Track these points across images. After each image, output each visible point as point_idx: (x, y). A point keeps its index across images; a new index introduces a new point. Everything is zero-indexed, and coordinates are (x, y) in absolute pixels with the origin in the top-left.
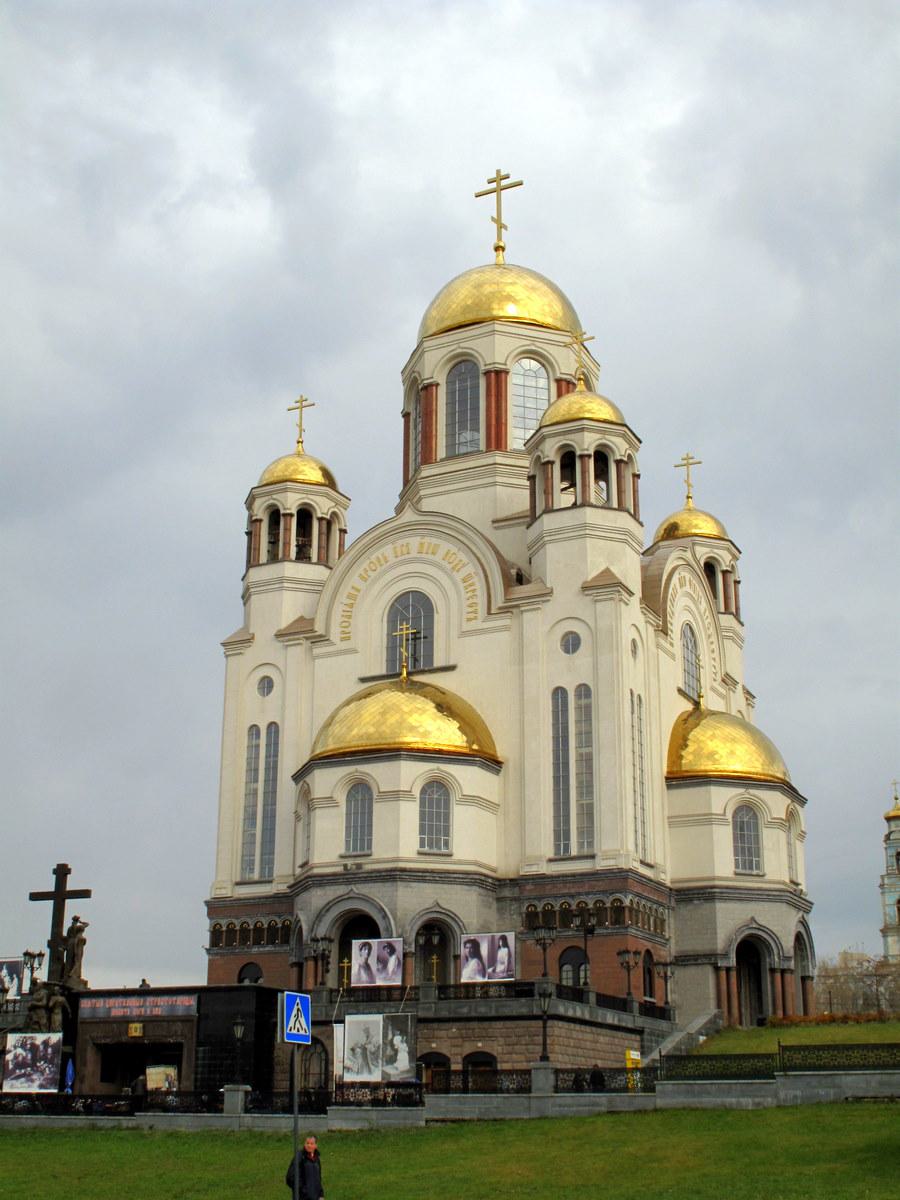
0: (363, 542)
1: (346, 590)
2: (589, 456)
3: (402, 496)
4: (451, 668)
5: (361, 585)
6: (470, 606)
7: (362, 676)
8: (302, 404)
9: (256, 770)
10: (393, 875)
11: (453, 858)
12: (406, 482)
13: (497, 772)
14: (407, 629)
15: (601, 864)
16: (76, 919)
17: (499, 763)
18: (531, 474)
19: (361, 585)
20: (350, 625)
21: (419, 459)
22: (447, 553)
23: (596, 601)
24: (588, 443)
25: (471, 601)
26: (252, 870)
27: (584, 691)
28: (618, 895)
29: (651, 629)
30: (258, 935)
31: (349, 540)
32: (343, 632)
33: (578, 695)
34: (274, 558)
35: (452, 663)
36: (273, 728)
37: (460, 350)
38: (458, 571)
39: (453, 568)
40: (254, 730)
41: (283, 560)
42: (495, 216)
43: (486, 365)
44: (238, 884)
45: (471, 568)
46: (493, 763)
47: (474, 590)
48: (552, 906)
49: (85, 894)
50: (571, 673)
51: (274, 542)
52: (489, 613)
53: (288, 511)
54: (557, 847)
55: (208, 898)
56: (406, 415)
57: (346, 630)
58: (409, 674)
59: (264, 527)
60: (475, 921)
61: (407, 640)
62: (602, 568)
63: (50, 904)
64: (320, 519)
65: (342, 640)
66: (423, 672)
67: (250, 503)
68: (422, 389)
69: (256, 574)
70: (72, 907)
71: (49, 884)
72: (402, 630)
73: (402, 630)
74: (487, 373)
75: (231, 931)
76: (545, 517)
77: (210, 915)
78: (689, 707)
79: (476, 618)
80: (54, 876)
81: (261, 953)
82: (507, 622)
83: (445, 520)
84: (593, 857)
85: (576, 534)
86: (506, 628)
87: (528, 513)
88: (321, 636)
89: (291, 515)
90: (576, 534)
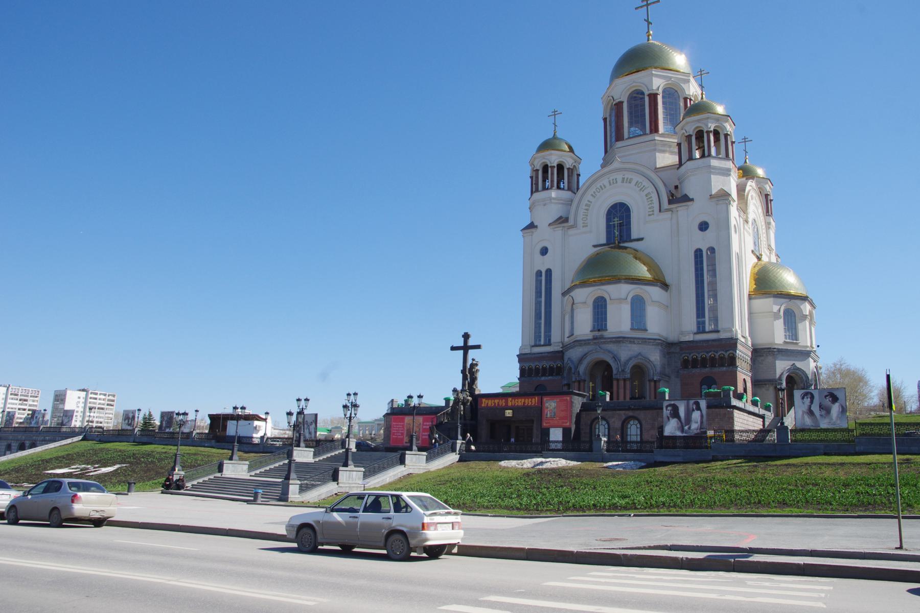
1: (585, 202)
2: (711, 131)
3: (604, 159)
4: (641, 239)
5: (591, 199)
6: (649, 208)
7: (595, 244)
8: (555, 113)
9: (541, 293)
10: (620, 340)
11: (648, 332)
12: (606, 152)
13: (667, 291)
14: (617, 221)
15: (723, 335)
16: (473, 360)
17: (667, 285)
18: (679, 142)
19: (591, 199)
20: (587, 219)
21: (614, 139)
22: (637, 183)
25: (650, 206)
26: (540, 340)
27: (712, 250)
28: (731, 352)
29: (741, 220)
30: (544, 371)
31: (582, 180)
32: (583, 223)
34: (544, 189)
35: (641, 237)
36: (549, 272)
37: (634, 84)
38: (643, 191)
39: (641, 189)
40: (539, 273)
42: (646, 19)
44: (533, 346)
45: (651, 189)
46: (665, 286)
47: (651, 201)
48: (724, 355)
49: (478, 347)
50: (703, 241)
51: (544, 181)
52: (660, 211)
53: (553, 165)
54: (698, 328)
55: (518, 354)
56: (605, 120)
57: (586, 222)
58: (619, 243)
59: (540, 173)
60: (659, 363)
61: (617, 226)
62: (719, 188)
63: (461, 352)
64: (568, 169)
65: (583, 227)
66: (626, 241)
67: (532, 164)
68: (615, 104)
69: (536, 195)
70: (472, 354)
71: (462, 344)
72: (615, 221)
73: (615, 221)
74: (650, 95)
75: (530, 369)
76: (688, 163)
77: (520, 361)
78: (756, 260)
79: (653, 214)
80: (463, 339)
84: (718, 331)
87: (678, 163)
89: (554, 167)
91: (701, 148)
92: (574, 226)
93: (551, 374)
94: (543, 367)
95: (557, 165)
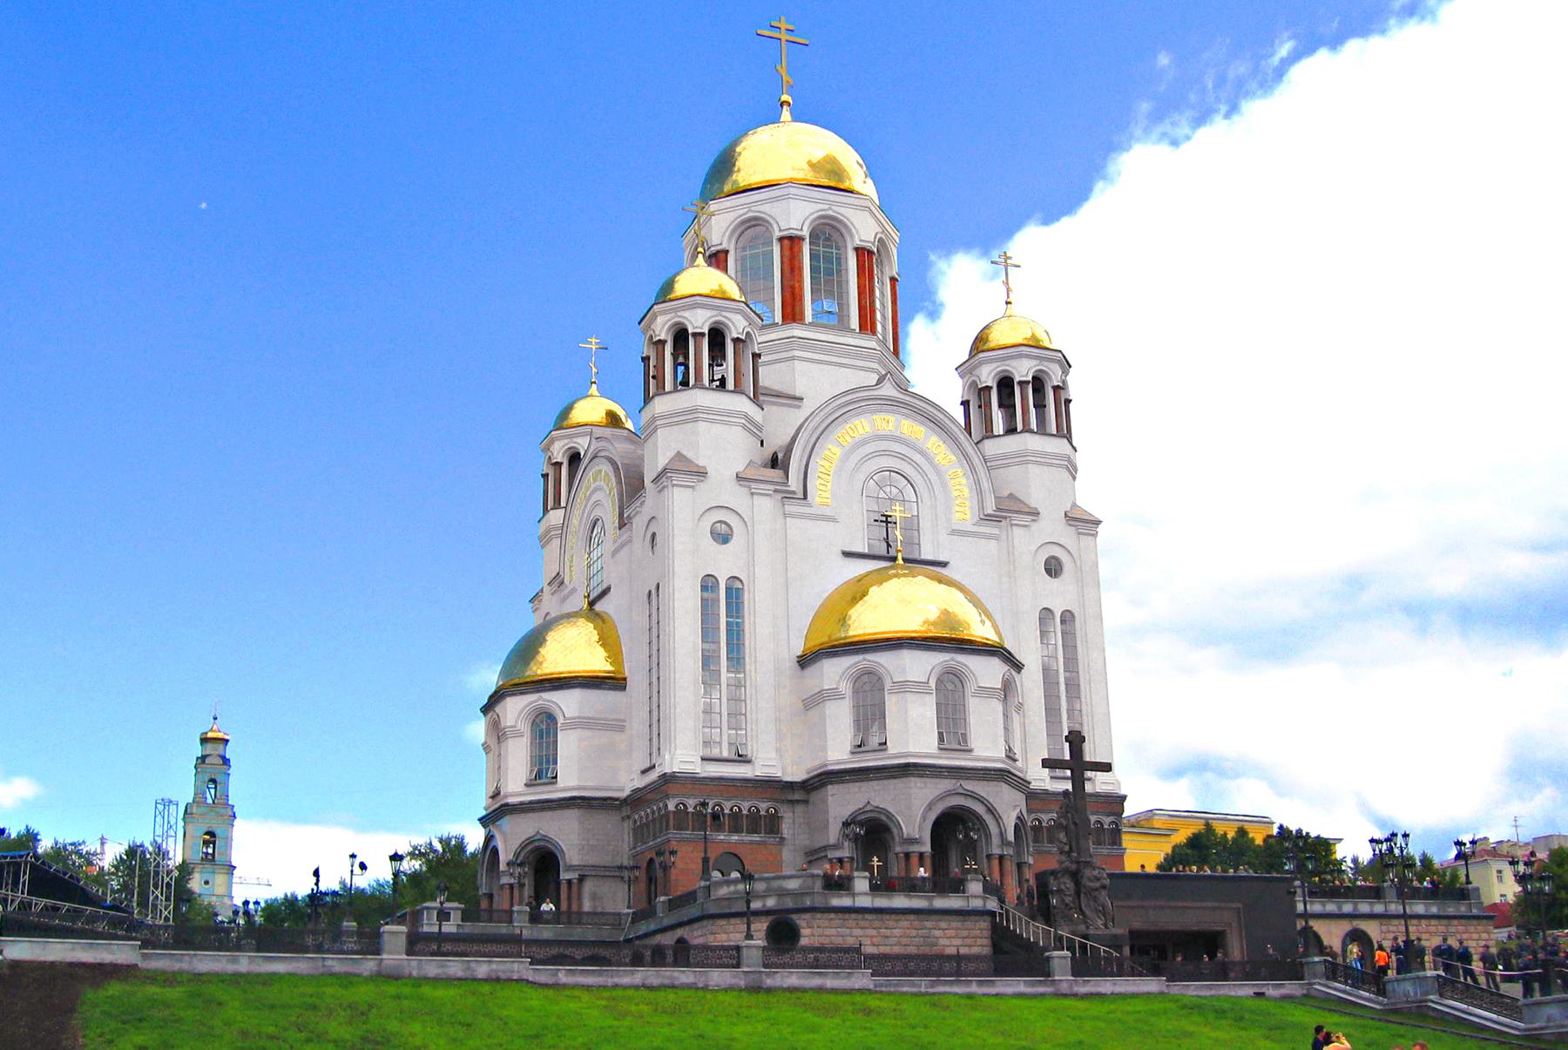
0: (834, 405)
4: (944, 564)
7: (847, 549)
23: (1080, 533)
24: (1023, 370)
27: (1068, 617)
33: (1063, 622)
35: (941, 558)
37: (830, 213)
41: (695, 387)
43: (861, 240)
81: (742, 843)
82: (996, 531)
83: (854, 396)
85: (1058, 462)
86: (997, 538)
88: (794, 492)
90: (1058, 462)
91: (1007, 404)
92: (788, 496)
93: (754, 830)
94: (767, 811)
95: (711, 330)
